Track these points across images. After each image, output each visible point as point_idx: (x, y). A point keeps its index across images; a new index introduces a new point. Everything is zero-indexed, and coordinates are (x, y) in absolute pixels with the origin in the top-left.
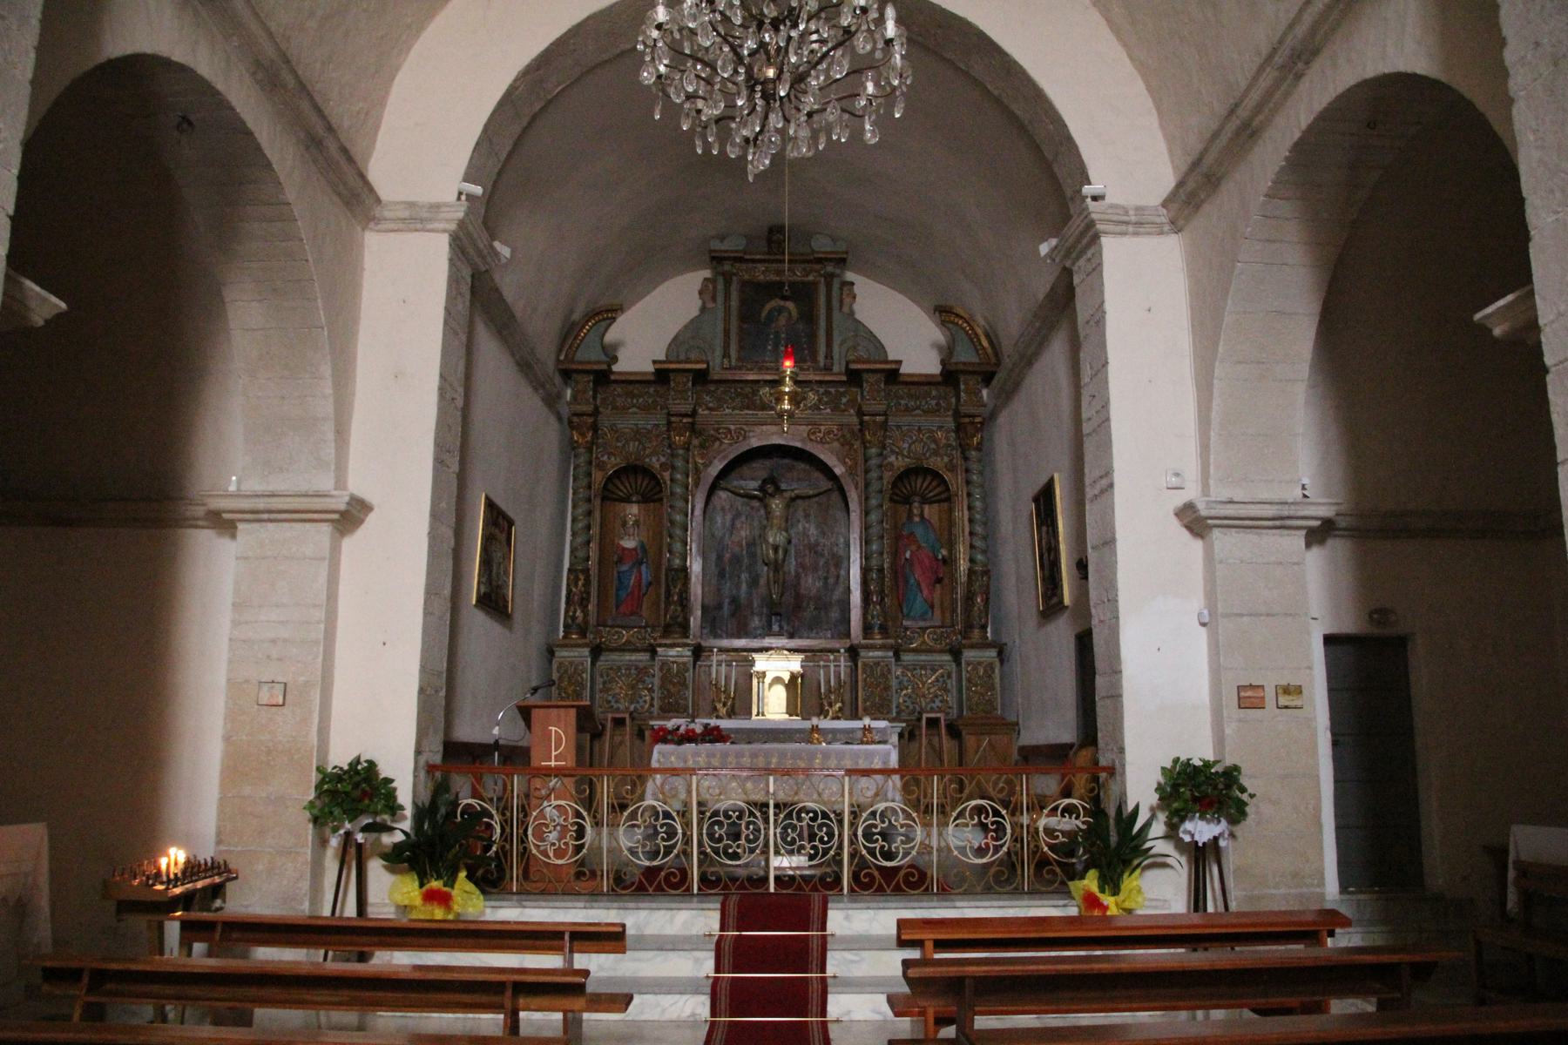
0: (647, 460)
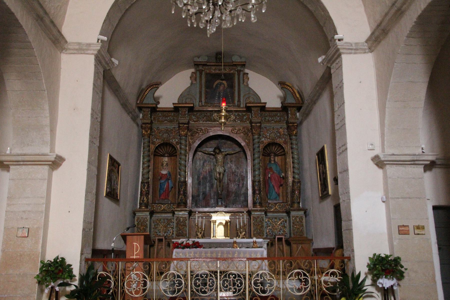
0: (171, 141)
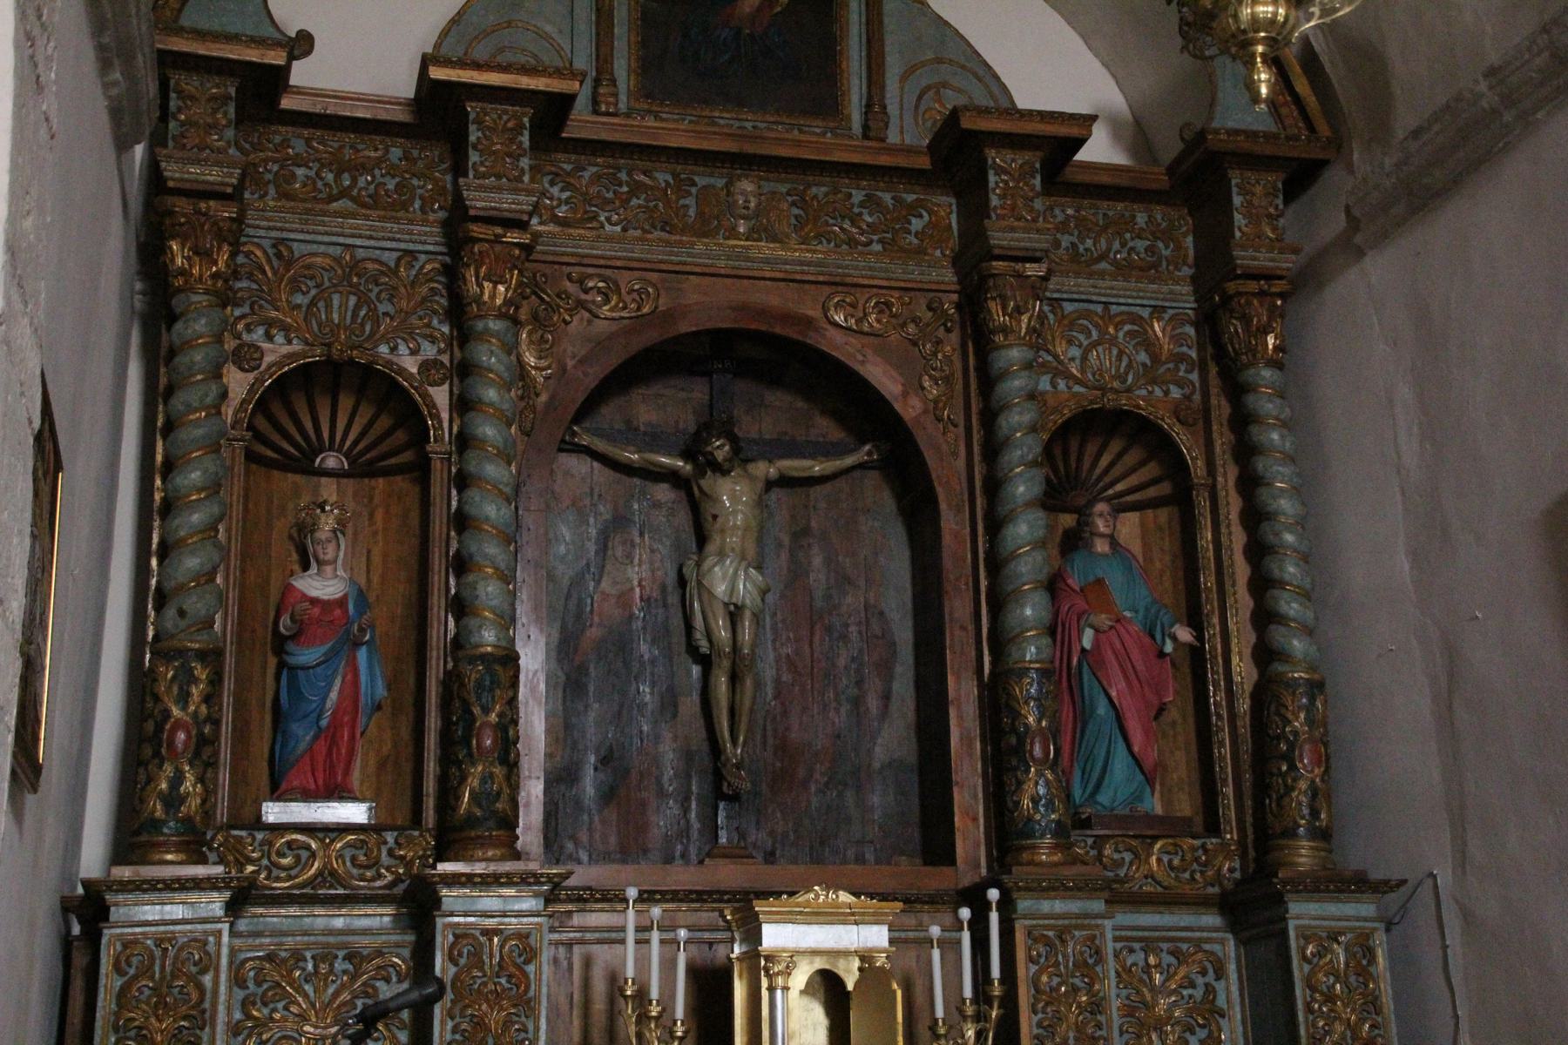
0: (383, 349)
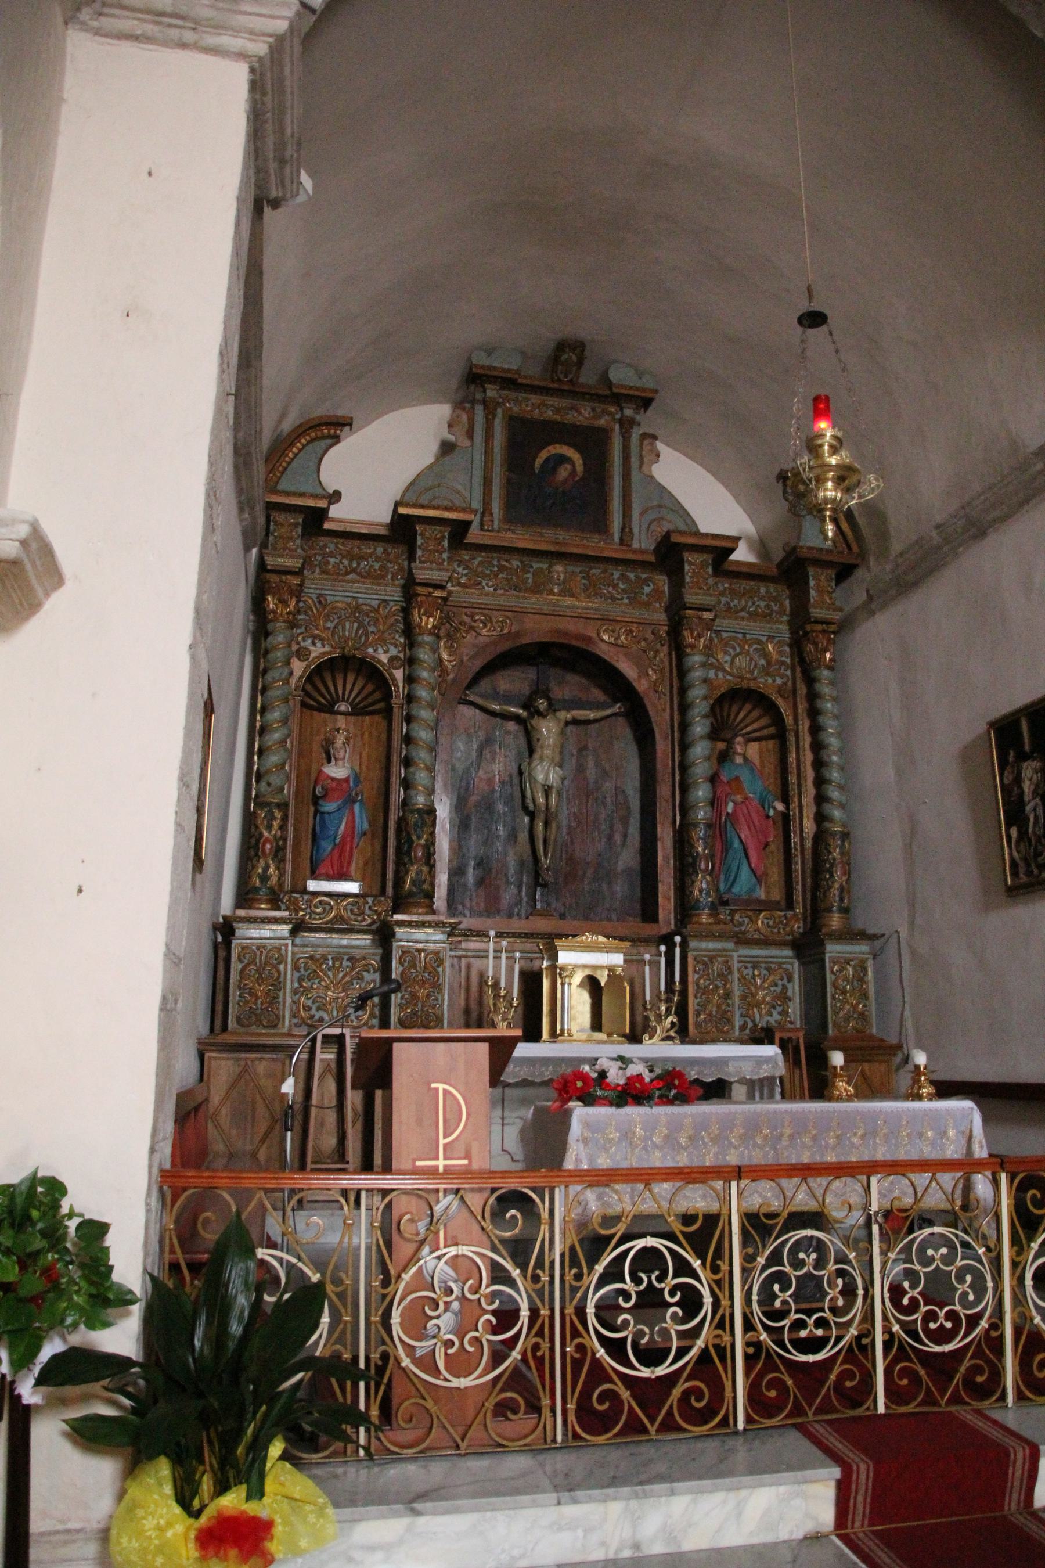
0: (370, 650)
